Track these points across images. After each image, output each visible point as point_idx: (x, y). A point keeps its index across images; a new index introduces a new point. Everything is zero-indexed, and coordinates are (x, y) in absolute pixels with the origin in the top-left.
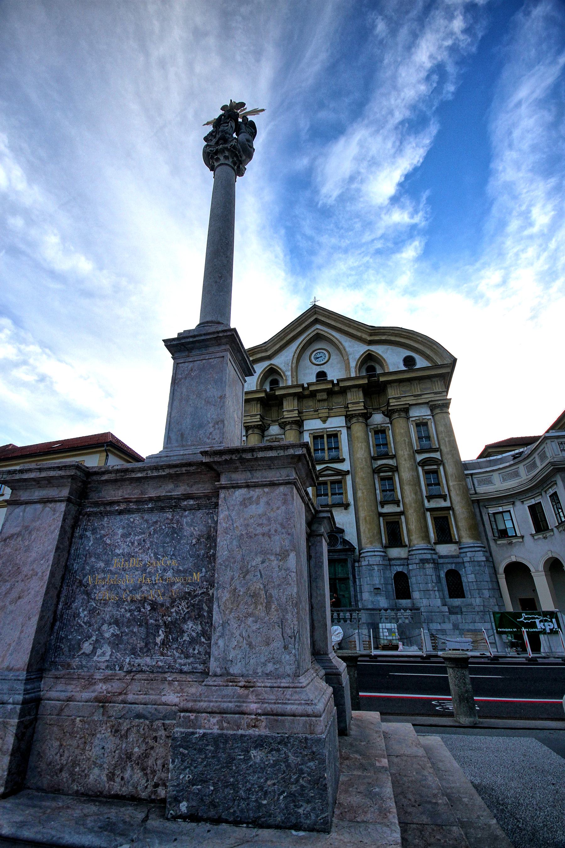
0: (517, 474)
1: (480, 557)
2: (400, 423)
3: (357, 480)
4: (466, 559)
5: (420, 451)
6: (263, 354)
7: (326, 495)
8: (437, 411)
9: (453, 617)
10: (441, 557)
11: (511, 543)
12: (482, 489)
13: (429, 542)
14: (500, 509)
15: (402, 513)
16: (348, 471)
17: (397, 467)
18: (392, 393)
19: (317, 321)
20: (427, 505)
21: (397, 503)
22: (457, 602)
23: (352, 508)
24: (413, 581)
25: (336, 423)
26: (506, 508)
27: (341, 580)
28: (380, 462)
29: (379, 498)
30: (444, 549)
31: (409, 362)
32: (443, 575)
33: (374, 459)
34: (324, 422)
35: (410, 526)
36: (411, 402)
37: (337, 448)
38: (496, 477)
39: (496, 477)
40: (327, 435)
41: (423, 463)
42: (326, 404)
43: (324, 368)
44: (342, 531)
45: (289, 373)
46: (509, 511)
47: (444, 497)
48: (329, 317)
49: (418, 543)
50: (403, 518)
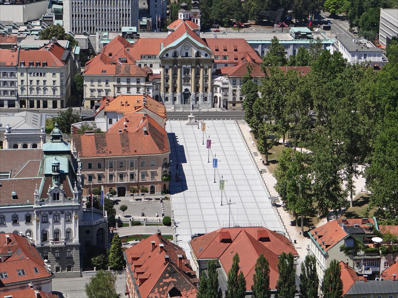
25: (189, 66)
35: (201, 90)
43: (187, 51)
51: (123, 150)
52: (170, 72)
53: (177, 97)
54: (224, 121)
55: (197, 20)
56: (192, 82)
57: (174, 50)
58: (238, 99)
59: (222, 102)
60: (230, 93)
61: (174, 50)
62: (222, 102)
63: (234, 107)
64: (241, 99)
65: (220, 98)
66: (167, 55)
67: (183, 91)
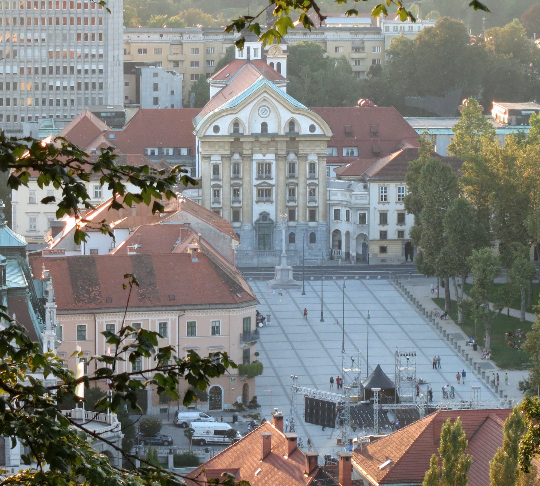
0: (346, 195)
1: (324, 229)
2: (303, 163)
3: (279, 191)
4: (319, 229)
5: (310, 178)
6: (233, 112)
7: (263, 196)
8: (321, 159)
9: (310, 251)
10: (309, 227)
11: (337, 222)
12: (332, 198)
13: (306, 221)
14: (337, 208)
15: (297, 206)
16: (274, 185)
17: (297, 184)
18: (301, 146)
19: (265, 91)
20: (308, 205)
21: (295, 201)
22: (312, 244)
23: (274, 203)
24: (297, 236)
25: (270, 157)
26: (339, 208)
27: (266, 235)
28: (291, 181)
29: (287, 199)
30: (312, 224)
31: (312, 128)
32: (309, 235)
33: (287, 178)
34: (264, 156)
35: (300, 214)
36: (308, 153)
37: (270, 172)
38: (339, 194)
39: (339, 194)
40: (266, 164)
41: (309, 185)
42: (266, 147)
43: (267, 121)
44: (269, 214)
45: (247, 125)
46: (340, 210)
47: (315, 201)
48: (273, 92)
49: (301, 221)
50: (297, 208)
51: (141, 295)
52: (226, 172)
53: (242, 234)
54: (364, 281)
55: (279, 65)
56: (279, 194)
57: (233, 117)
58: (392, 234)
59: (353, 243)
60: (374, 219)
61: (233, 117)
62: (353, 243)
63: (384, 255)
64: (401, 234)
65: (348, 233)
66: (216, 129)
67: (256, 217)
